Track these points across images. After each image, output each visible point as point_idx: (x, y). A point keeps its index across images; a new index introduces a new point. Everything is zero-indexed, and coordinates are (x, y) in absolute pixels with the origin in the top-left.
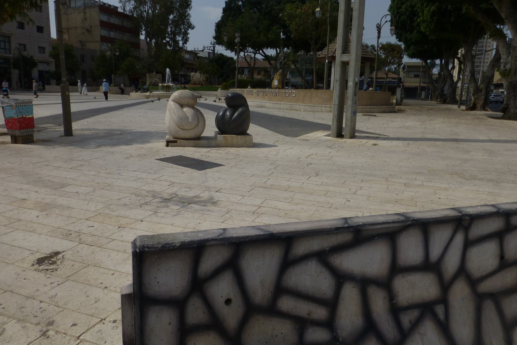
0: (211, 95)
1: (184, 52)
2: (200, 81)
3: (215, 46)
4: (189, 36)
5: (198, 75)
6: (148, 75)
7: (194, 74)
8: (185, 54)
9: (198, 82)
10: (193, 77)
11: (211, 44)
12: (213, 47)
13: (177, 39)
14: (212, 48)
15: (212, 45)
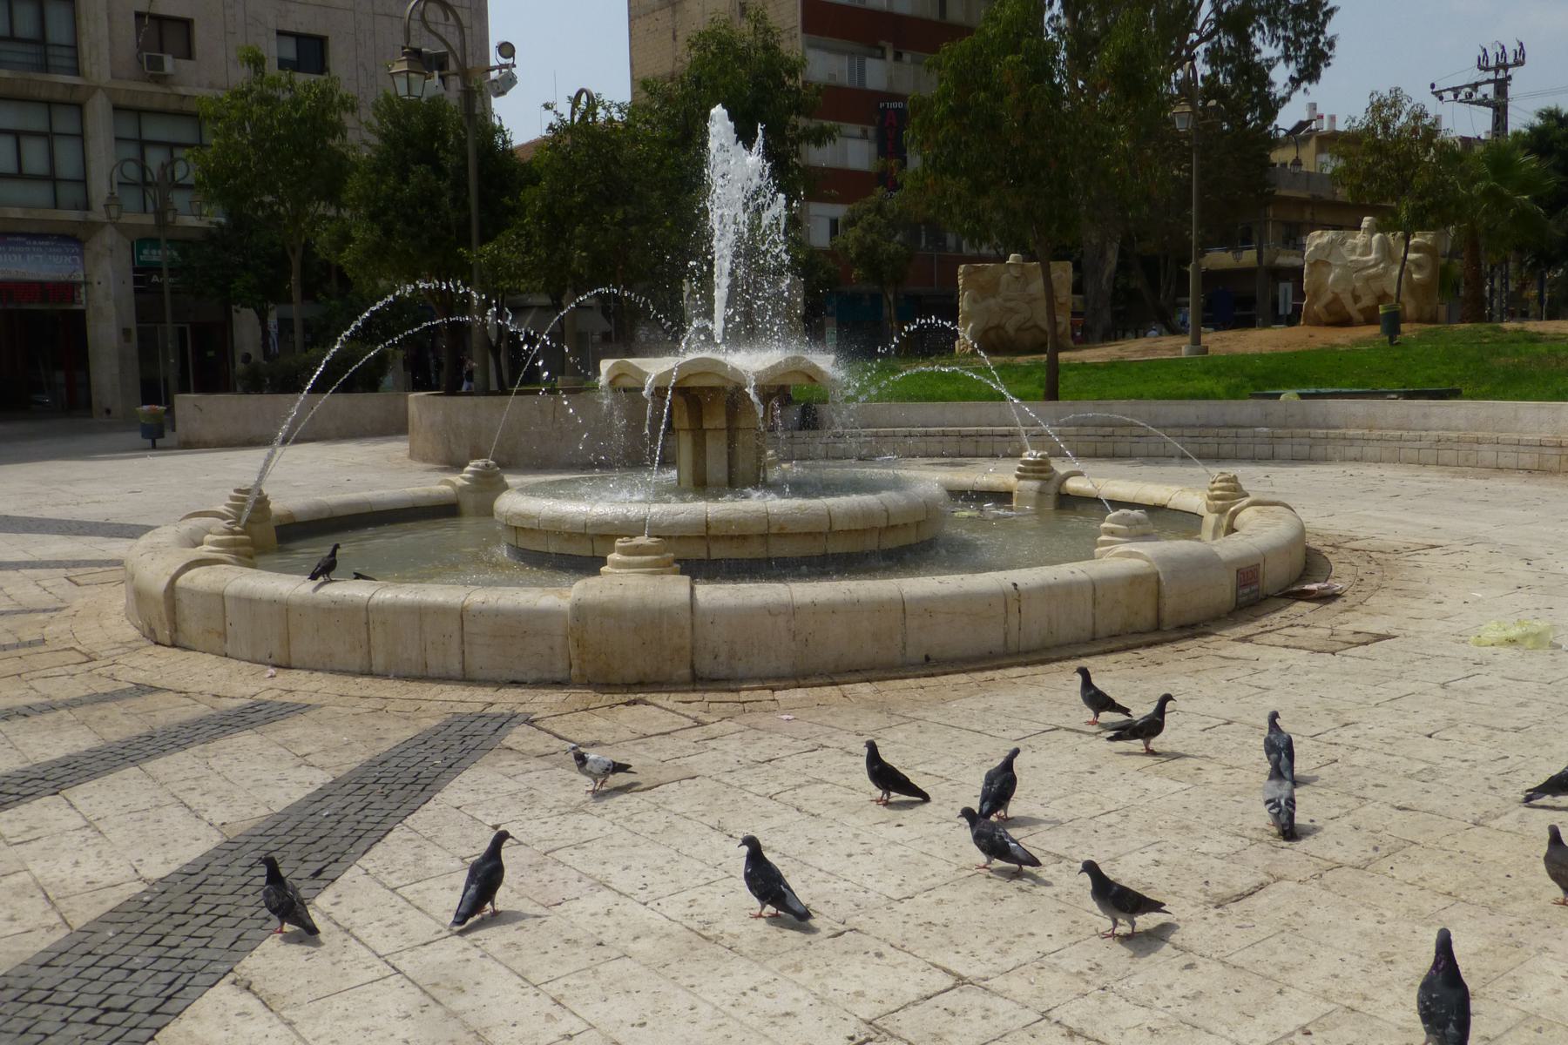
0: (1487, 454)
1: (1313, 143)
2: (1383, 297)
3: (1509, 78)
4: (1330, 29)
5: (1367, 249)
6: (967, 274)
7: (1332, 242)
8: (1321, 150)
9: (1367, 301)
10: (1321, 264)
11: (1480, 67)
12: (1492, 86)
13: (1257, 58)
14: (1489, 90)
15: (1491, 75)
